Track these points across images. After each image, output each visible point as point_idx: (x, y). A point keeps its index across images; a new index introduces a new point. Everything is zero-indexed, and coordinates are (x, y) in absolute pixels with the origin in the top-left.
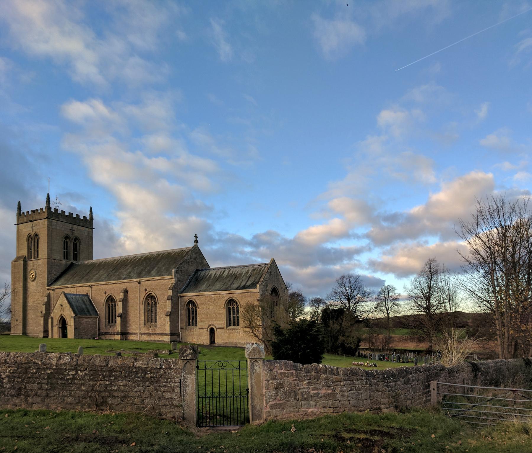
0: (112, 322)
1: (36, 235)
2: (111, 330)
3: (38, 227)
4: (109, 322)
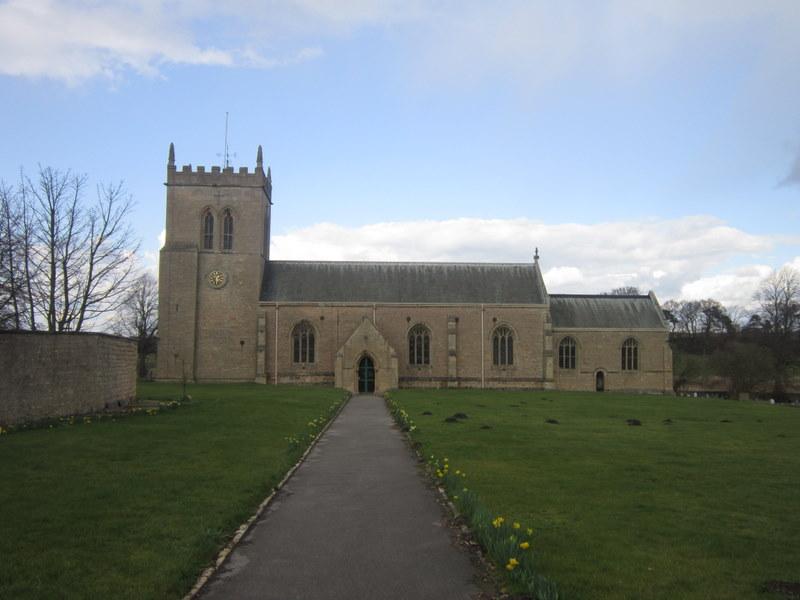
0: (419, 362)
1: (227, 211)
2: (420, 374)
3: (235, 199)
4: (412, 361)
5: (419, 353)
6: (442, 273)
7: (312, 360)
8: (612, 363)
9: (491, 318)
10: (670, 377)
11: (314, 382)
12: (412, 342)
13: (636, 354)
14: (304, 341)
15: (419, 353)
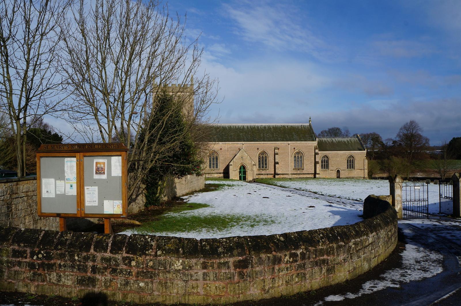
0: (263, 167)
5: (263, 163)
6: (271, 128)
7: (217, 167)
8: (343, 166)
9: (293, 148)
10: (366, 171)
11: (218, 176)
12: (259, 159)
13: (352, 163)
14: (213, 159)
15: (263, 163)
